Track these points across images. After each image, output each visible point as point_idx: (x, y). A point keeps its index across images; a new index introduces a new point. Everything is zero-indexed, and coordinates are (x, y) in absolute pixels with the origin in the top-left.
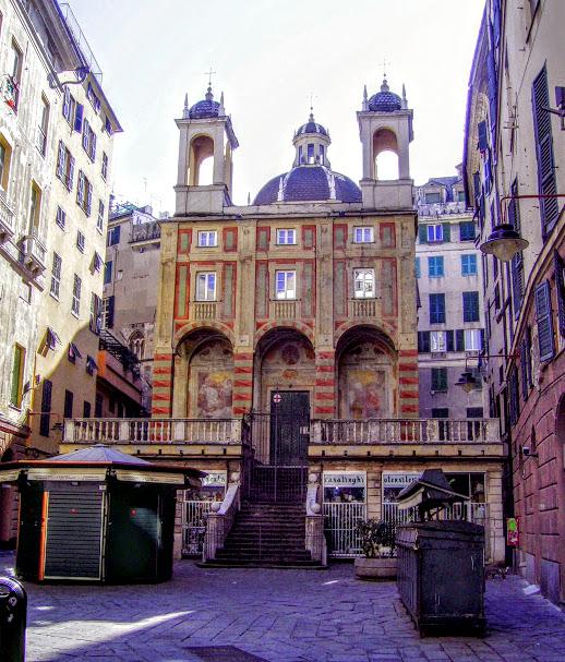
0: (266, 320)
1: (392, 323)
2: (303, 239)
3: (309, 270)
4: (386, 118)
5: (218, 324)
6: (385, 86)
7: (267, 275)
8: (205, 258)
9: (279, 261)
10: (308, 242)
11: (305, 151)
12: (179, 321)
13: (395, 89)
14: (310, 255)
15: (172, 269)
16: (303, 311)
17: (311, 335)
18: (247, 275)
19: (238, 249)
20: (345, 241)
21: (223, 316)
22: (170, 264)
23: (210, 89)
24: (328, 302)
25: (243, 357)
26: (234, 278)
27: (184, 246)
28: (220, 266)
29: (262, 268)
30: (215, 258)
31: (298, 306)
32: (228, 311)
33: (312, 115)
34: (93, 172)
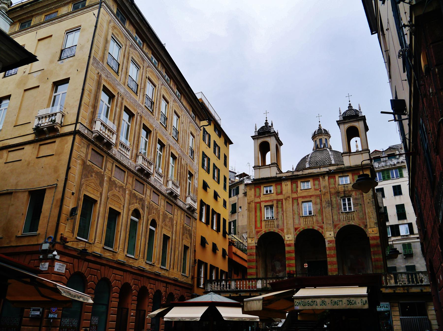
1: (363, 223)
2: (314, 185)
3: (318, 200)
4: (353, 122)
6: (350, 106)
7: (298, 204)
8: (267, 199)
9: (303, 197)
10: (317, 187)
11: (318, 142)
12: (259, 230)
13: (355, 107)
14: (318, 193)
15: (253, 205)
17: (322, 232)
18: (288, 205)
19: (283, 193)
20: (335, 184)
22: (252, 203)
23: (266, 120)
24: (330, 215)
25: (289, 245)
26: (282, 207)
27: (258, 195)
28: (275, 202)
29: (295, 201)
30: (272, 199)
31: (314, 218)
33: (320, 125)
34: (220, 164)
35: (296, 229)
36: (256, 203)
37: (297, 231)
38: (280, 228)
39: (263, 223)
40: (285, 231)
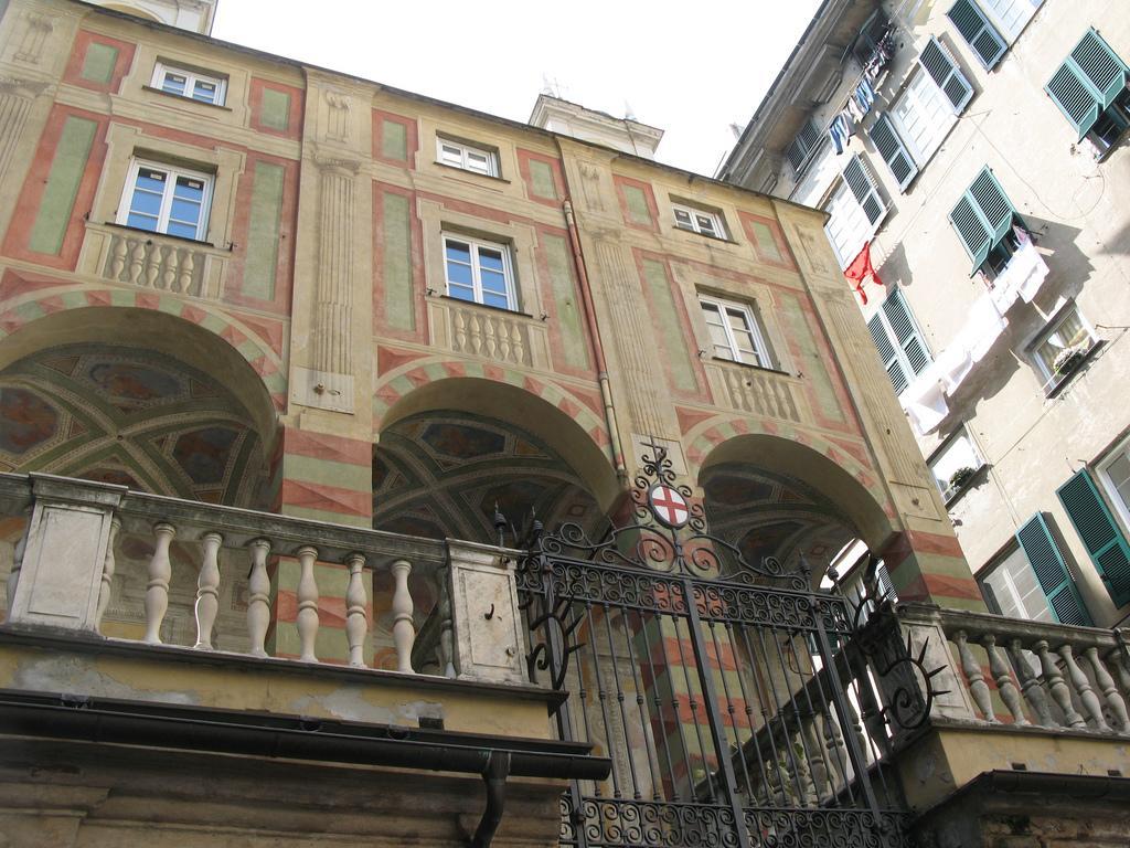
0: (419, 347)
5: (215, 317)
8: (169, 123)
9: (449, 202)
16: (556, 349)
21: (233, 293)
25: (325, 449)
30: (217, 134)
32: (259, 283)
35: (387, 360)
36: (61, 111)
37: (394, 373)
38: (244, 311)
39: (94, 244)
40: (301, 339)
